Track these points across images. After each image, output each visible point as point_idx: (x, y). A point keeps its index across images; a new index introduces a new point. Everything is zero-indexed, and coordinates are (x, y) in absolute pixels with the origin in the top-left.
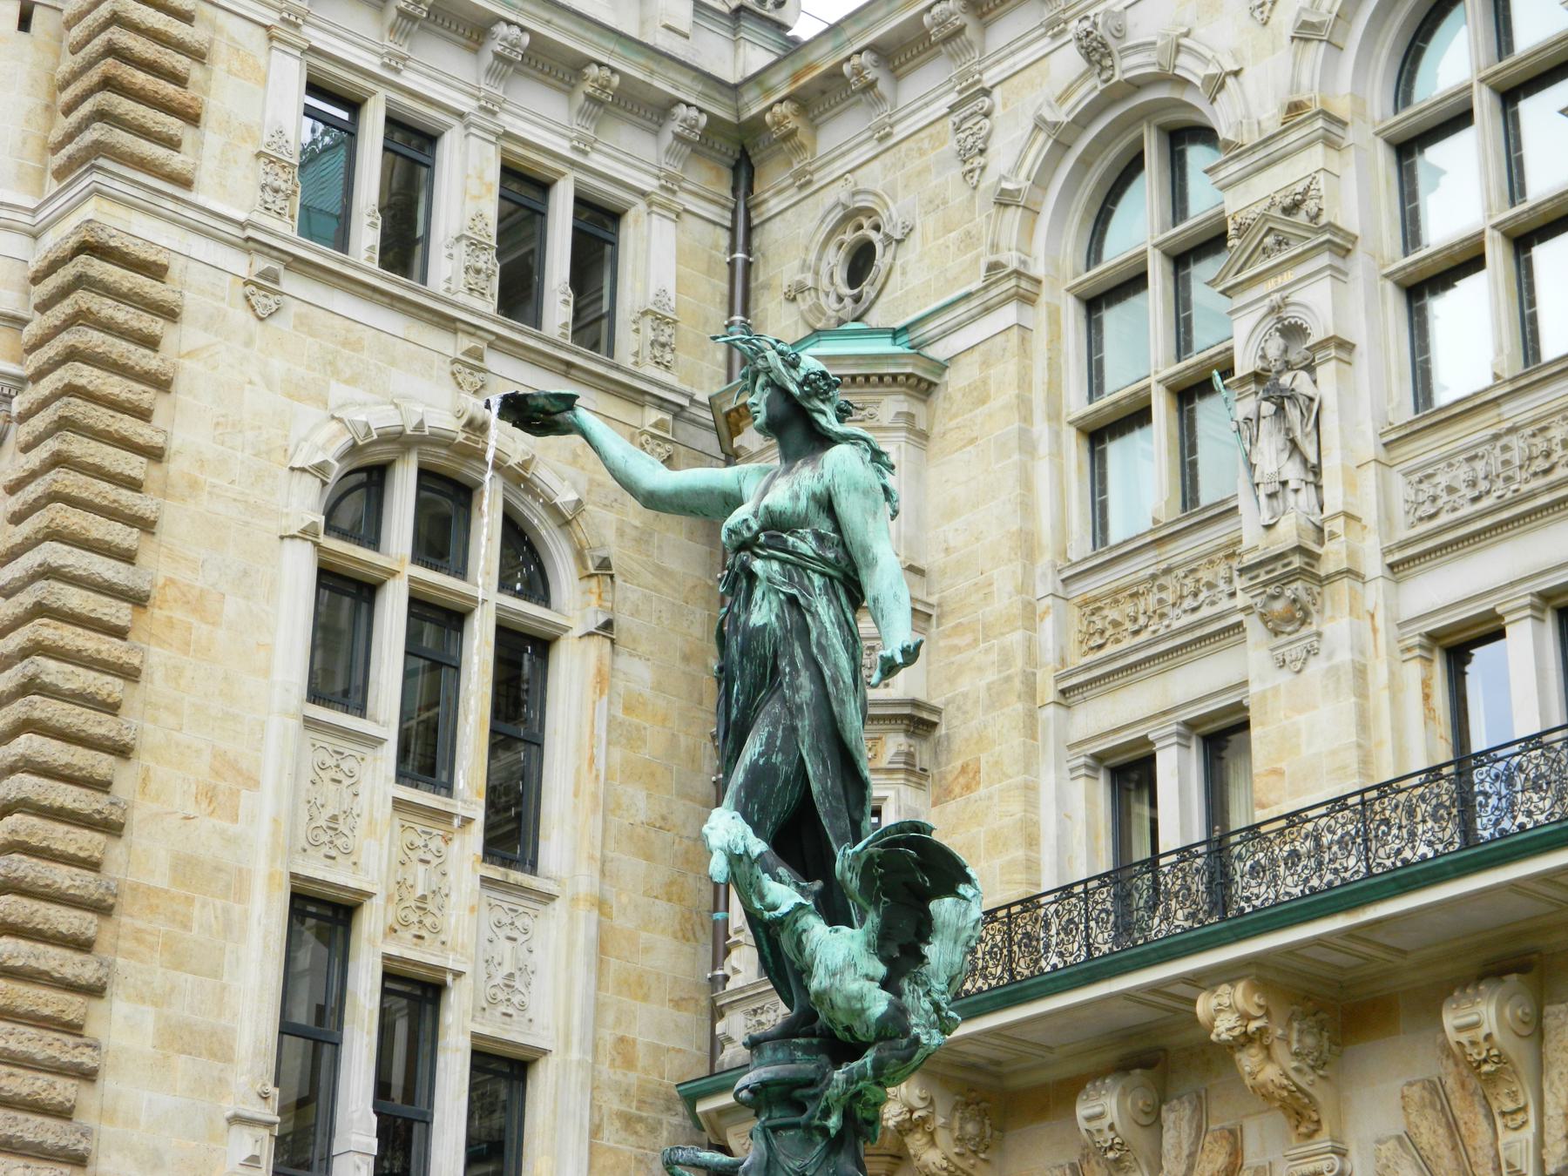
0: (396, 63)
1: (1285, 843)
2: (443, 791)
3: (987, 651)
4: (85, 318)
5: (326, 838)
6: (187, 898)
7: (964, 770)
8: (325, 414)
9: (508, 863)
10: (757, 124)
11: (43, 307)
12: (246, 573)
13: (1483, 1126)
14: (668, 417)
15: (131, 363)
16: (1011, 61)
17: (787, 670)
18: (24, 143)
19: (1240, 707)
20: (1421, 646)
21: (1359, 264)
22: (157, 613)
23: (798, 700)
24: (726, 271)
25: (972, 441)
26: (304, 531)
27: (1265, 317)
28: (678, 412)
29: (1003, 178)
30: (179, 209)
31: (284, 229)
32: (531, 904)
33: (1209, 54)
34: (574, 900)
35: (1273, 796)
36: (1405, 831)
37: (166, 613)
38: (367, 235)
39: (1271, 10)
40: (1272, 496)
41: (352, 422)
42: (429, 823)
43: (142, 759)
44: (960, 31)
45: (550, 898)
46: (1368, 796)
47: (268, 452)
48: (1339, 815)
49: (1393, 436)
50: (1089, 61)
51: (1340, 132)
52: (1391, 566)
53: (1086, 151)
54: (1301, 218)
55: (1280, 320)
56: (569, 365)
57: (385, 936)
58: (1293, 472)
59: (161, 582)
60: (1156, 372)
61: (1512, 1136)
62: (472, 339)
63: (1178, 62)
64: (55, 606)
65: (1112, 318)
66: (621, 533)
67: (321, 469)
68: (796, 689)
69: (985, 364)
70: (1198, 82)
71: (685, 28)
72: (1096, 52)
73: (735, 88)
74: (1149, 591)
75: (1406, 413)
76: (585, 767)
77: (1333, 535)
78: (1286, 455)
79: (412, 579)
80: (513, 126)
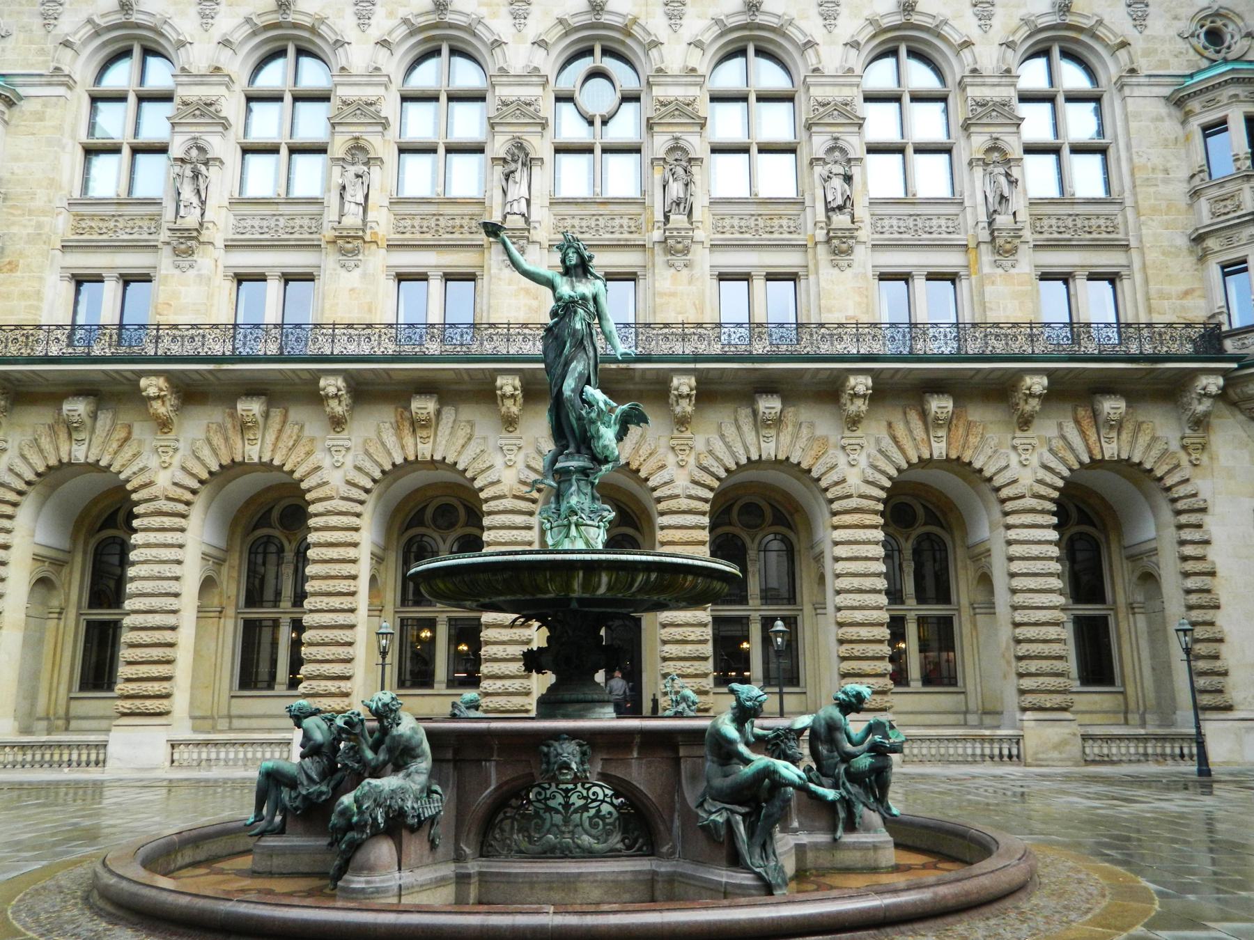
3: (30, 220)
7: (10, 263)
13: (239, 442)
25: (34, 134)
29: (67, 35)
35: (165, 312)
53: (107, 41)
58: (195, 201)
61: (250, 447)
69: (45, 105)
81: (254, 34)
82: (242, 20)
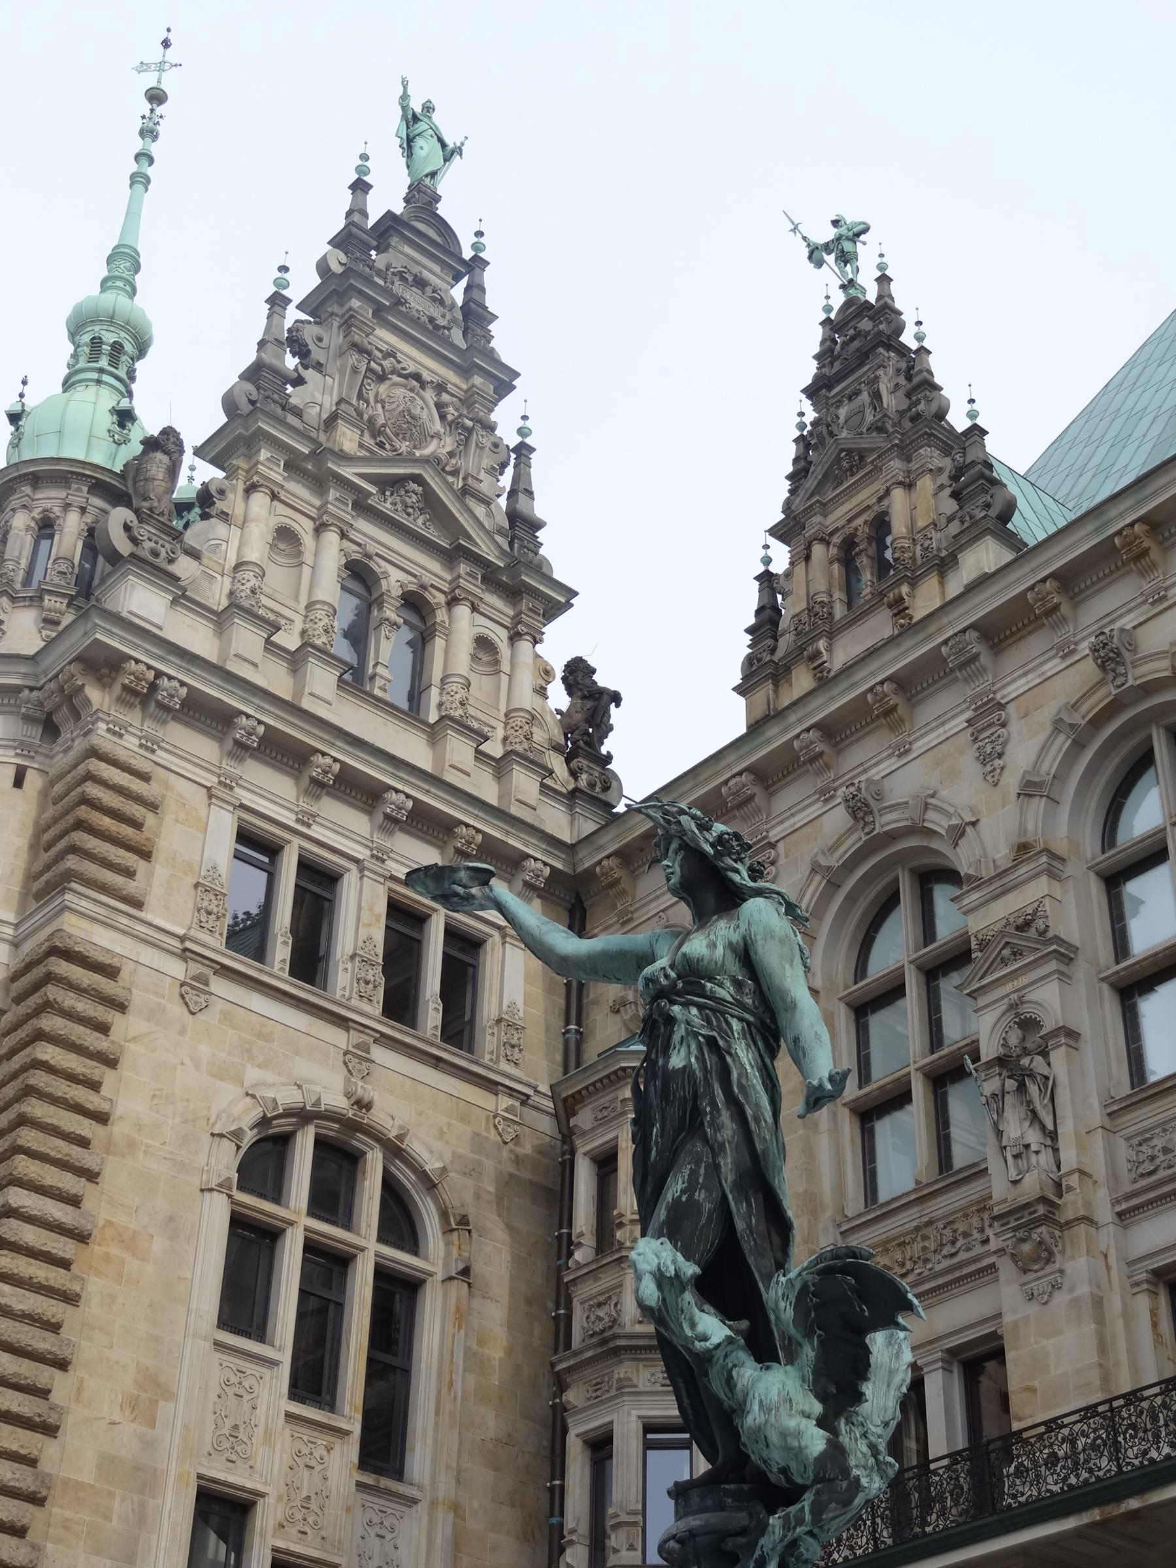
0: (308, 819)
1: (1045, 1447)
2: (327, 1408)
4: (52, 1007)
5: (228, 1445)
6: (109, 1492)
8: (241, 1091)
9: (379, 1472)
10: (589, 874)
11: (19, 1000)
12: (171, 1219)
14: (517, 1104)
15: (86, 1044)
16: (792, 821)
17: (708, 1109)
18: (12, 873)
19: (995, 1336)
20: (1147, 1281)
21: (1081, 970)
22: (96, 1249)
23: (720, 1138)
24: (563, 990)
26: (220, 1185)
27: (1004, 1014)
28: (525, 1100)
30: (132, 923)
31: (214, 943)
32: (397, 1507)
33: (951, 810)
34: (433, 1504)
36: (1150, 1434)
37: (104, 1249)
38: (281, 951)
39: (1000, 774)
40: (1016, 1157)
41: (263, 1098)
42: (315, 1434)
43: (77, 1371)
44: (751, 798)
45: (414, 1501)
46: (1115, 1404)
47: (194, 1121)
48: (1091, 1421)
49: (1116, 1107)
50: (855, 818)
51: (1060, 866)
52: (1119, 1214)
54: (1032, 933)
55: (1017, 1015)
56: (438, 1059)
57: (275, 1530)
58: (1033, 1137)
59: (101, 1223)
60: (915, 1062)
62: (362, 1035)
63: (926, 817)
64: (13, 1239)
65: (878, 1022)
66: (477, 1196)
67: (237, 1135)
68: (717, 1128)
70: (944, 833)
71: (533, 803)
72: (859, 810)
73: (573, 846)
74: (914, 1240)
75: (1125, 1089)
76: (445, 1390)
77: (1070, 1189)
78: (1027, 1123)
79: (306, 1229)
80: (396, 870)
81: (1078, 745)
82: (1049, 728)
